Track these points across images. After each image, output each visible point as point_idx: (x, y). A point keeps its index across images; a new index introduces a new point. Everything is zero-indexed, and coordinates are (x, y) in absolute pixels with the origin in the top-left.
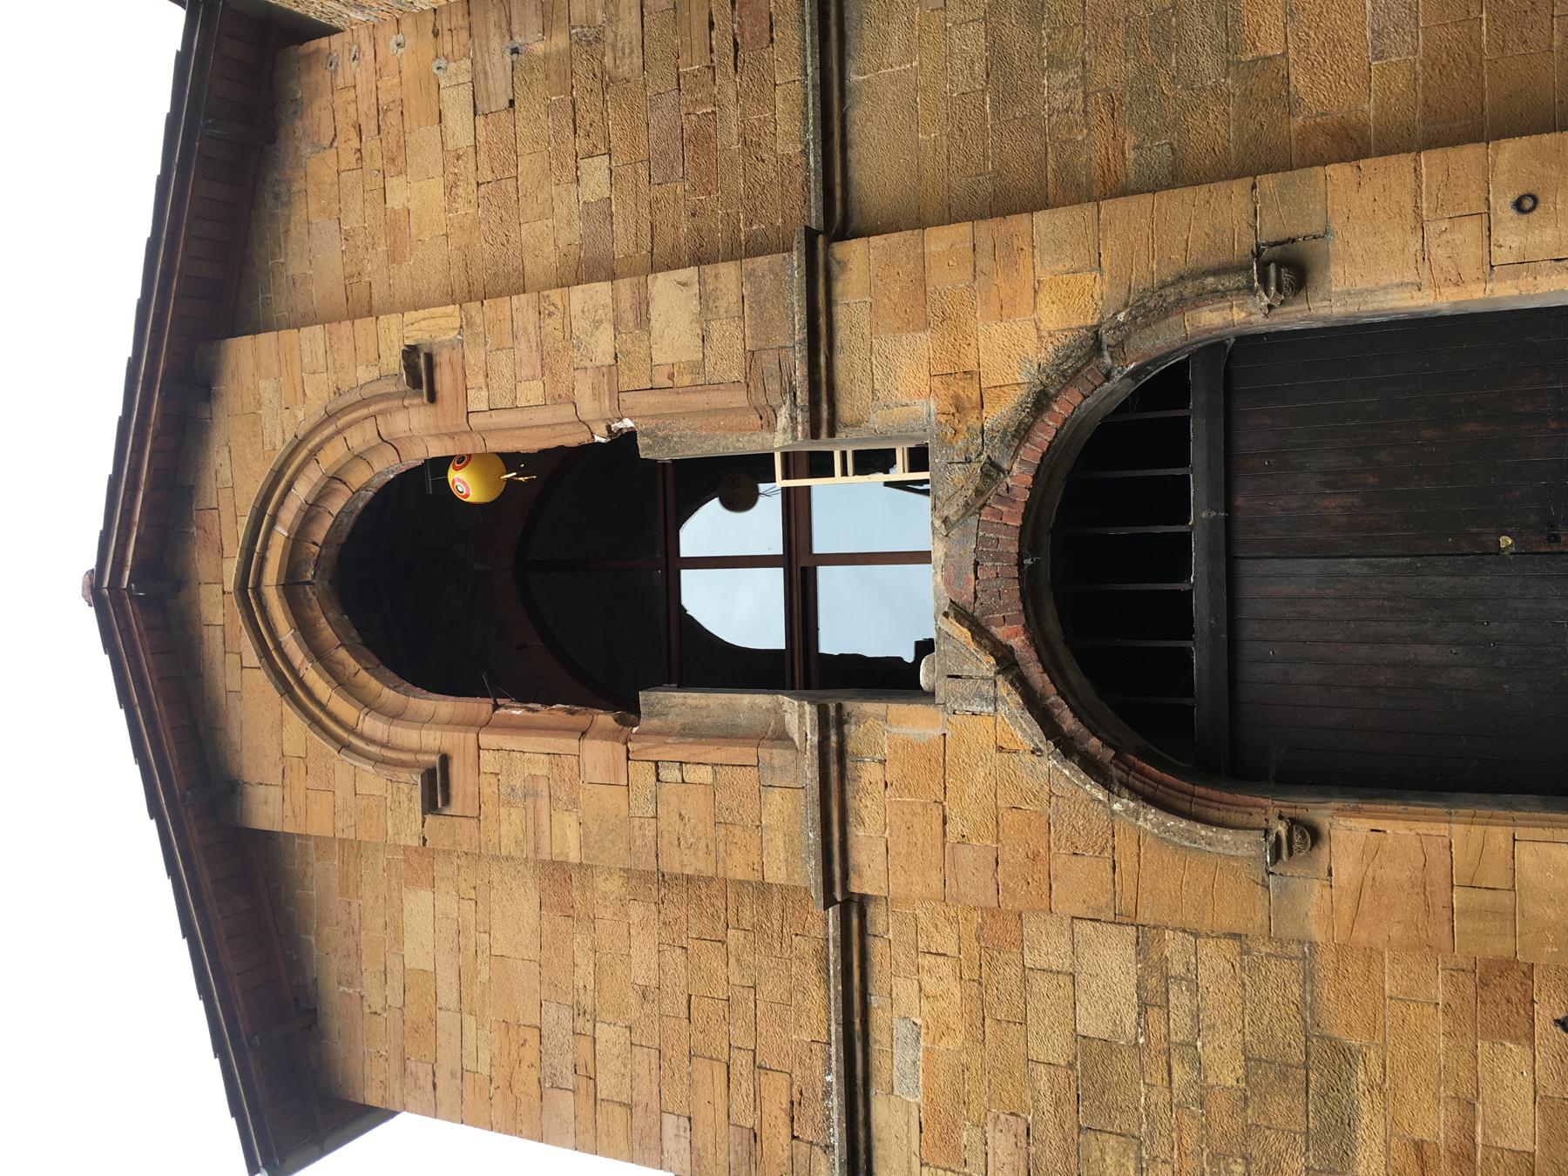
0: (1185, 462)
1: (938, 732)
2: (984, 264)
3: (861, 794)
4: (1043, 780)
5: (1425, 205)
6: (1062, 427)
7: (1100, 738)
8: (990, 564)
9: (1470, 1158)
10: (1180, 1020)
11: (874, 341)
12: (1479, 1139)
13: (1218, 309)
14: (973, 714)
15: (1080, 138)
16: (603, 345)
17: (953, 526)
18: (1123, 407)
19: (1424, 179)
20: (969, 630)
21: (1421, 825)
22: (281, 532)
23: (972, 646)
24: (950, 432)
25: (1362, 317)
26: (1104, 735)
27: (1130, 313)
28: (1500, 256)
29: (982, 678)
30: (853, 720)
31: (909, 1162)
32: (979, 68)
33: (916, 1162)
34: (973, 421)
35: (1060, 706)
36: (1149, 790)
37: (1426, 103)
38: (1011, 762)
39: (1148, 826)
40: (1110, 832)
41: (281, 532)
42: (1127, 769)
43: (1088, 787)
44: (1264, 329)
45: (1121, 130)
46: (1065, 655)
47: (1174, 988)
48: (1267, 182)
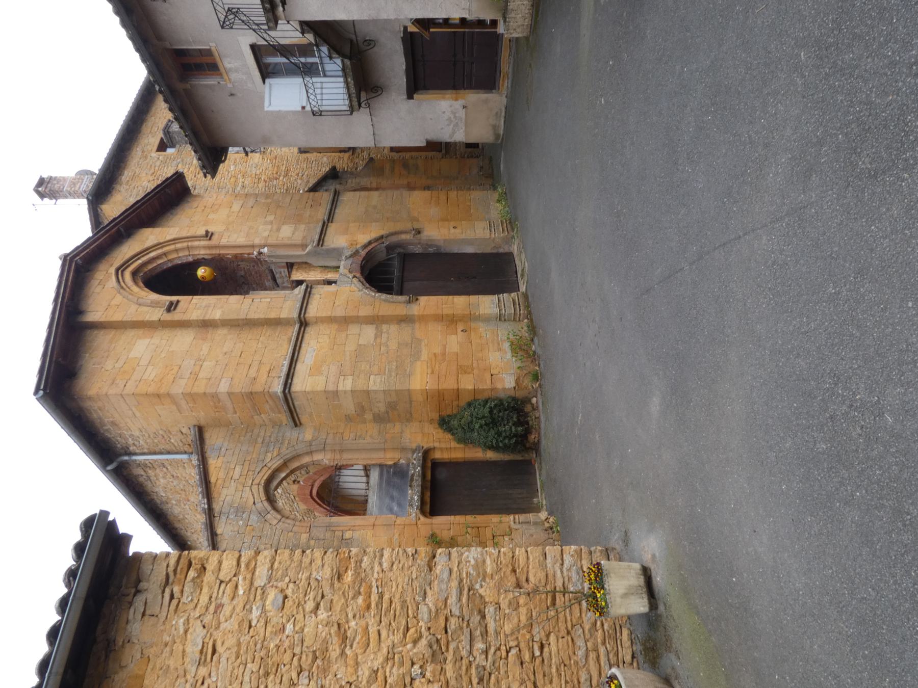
9: (445, 354)
10: (384, 340)
22: (140, 262)
31: (305, 376)
33: (307, 376)
34: (355, 246)
41: (140, 262)
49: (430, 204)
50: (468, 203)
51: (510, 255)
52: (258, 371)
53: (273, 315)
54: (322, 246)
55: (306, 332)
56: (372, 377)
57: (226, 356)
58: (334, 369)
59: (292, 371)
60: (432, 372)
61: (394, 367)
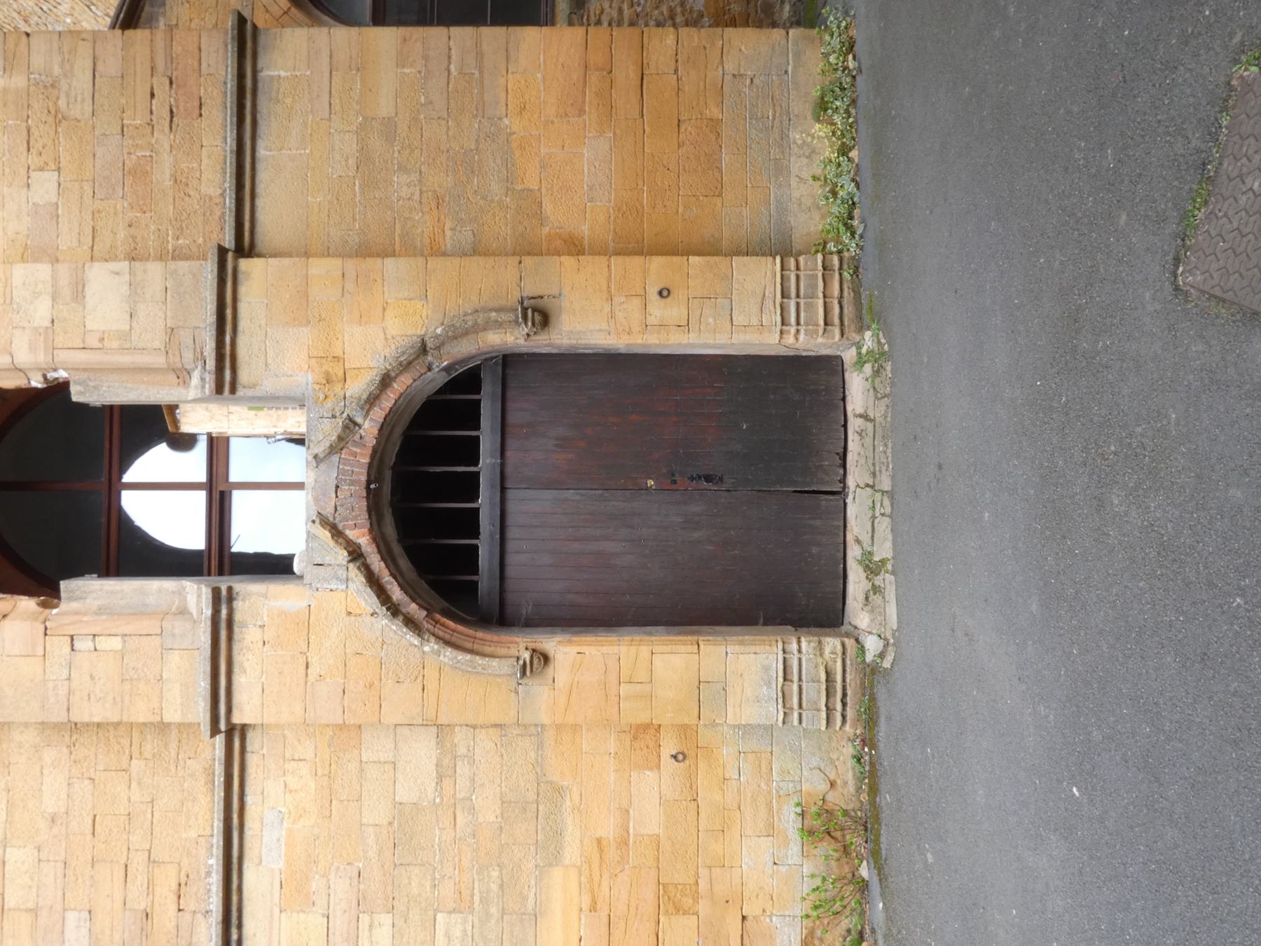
0: (477, 427)
1: (306, 604)
2: (350, 286)
3: (245, 651)
4: (378, 634)
5: (613, 287)
6: (400, 397)
7: (417, 604)
8: (347, 488)
9: (626, 844)
10: (463, 783)
11: (268, 329)
12: (631, 831)
13: (498, 333)
14: (331, 590)
15: (417, 218)
16: (42, 311)
17: (322, 460)
18: (439, 392)
19: (613, 272)
20: (330, 532)
21: (604, 648)
23: (332, 543)
24: (322, 397)
25: (577, 348)
26: (421, 602)
27: (444, 329)
28: (651, 320)
29: (338, 565)
30: (240, 598)
31: (271, 911)
32: (352, 162)
33: (277, 910)
34: (338, 389)
35: (391, 583)
36: (447, 637)
37: (615, 231)
38: (357, 623)
39: (446, 660)
40: (422, 666)
42: (434, 623)
43: (408, 636)
44: (524, 350)
45: (442, 217)
46: (397, 549)
47: (459, 764)
48: (528, 260)
49: (581, 112)
50: (714, 112)
51: (839, 360)
52: (150, 886)
53: (141, 713)
54: (233, 390)
55: (249, 748)
56: (439, 916)
57: (55, 830)
58: (342, 889)
59: (235, 898)
60: (593, 908)
61: (494, 887)
